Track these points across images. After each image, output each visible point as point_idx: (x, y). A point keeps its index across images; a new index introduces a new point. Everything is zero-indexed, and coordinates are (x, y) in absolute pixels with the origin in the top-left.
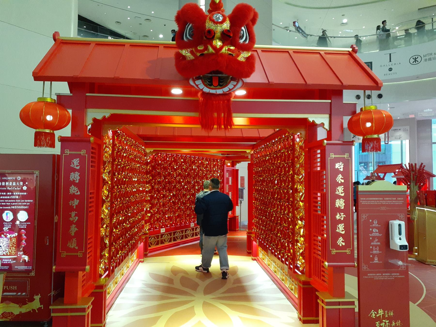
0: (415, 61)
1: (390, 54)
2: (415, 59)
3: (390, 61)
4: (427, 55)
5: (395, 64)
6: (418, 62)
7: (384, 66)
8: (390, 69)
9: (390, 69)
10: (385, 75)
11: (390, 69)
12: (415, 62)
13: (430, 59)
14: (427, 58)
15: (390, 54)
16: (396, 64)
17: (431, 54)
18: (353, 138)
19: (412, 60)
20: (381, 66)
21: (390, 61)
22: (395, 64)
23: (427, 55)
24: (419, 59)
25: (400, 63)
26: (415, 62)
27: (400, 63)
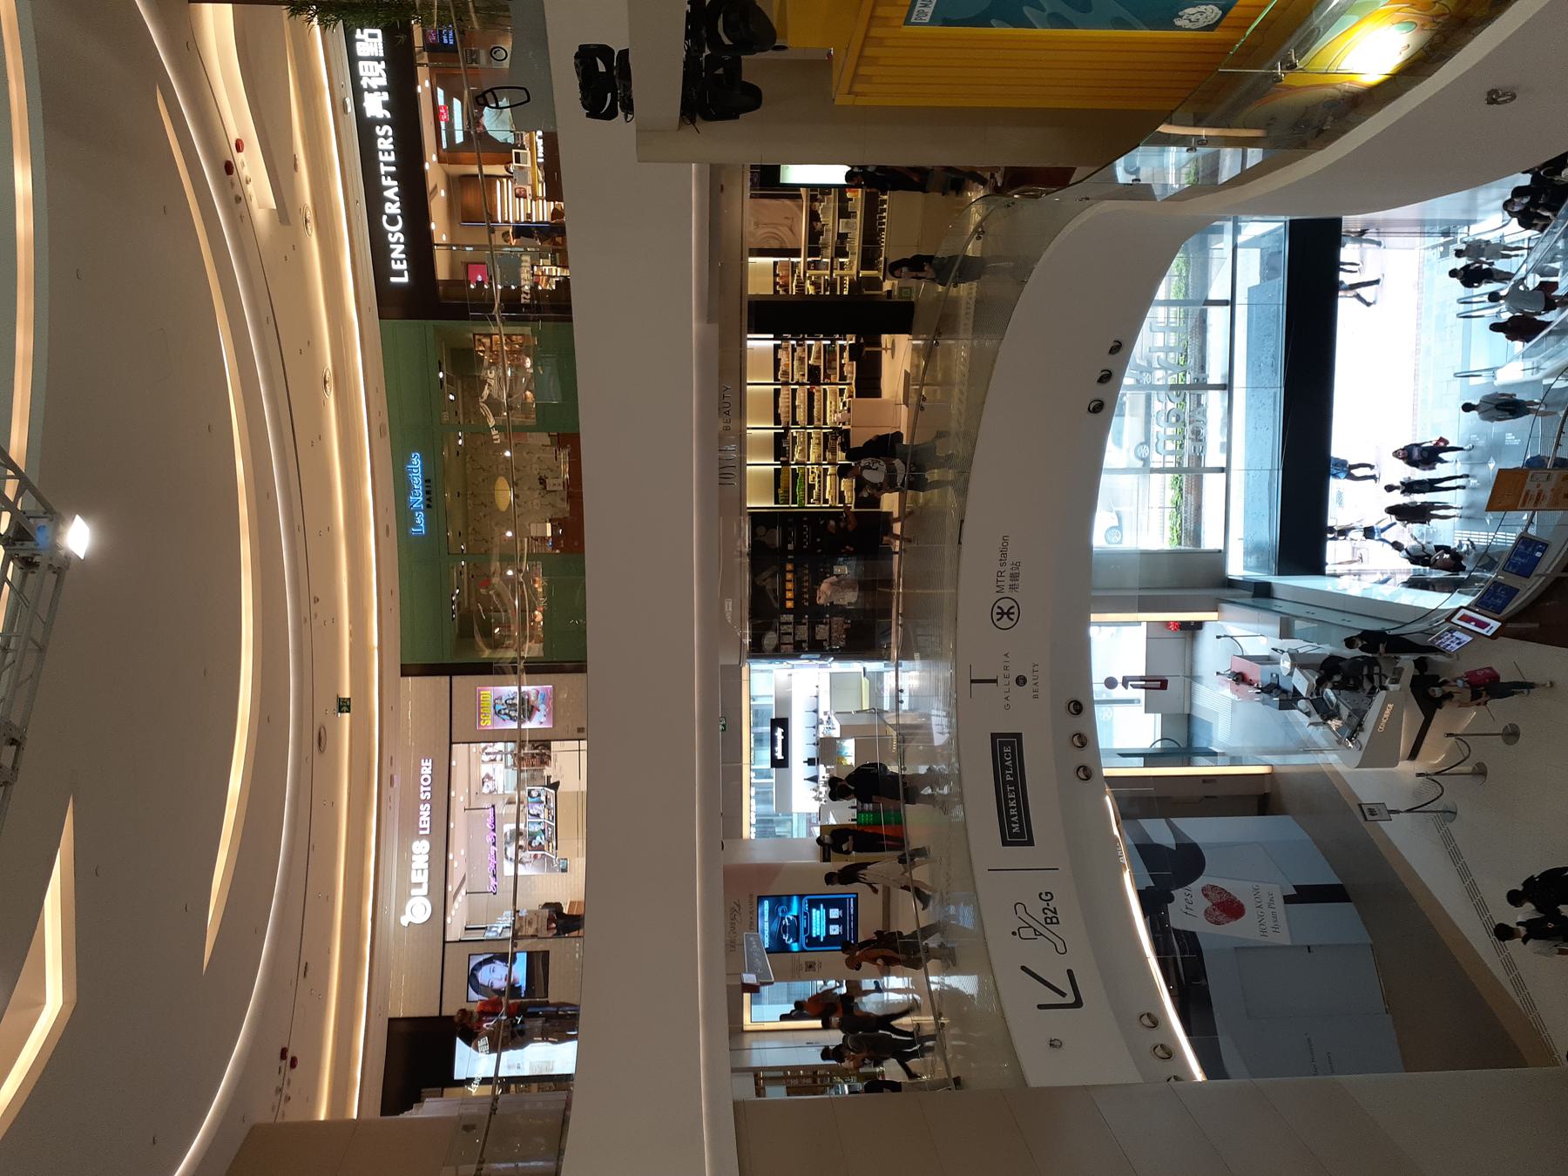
0: (1008, 613)
1: (972, 681)
2: (1008, 613)
3: (995, 681)
4: (999, 583)
5: (1006, 668)
6: (1013, 607)
7: (1007, 698)
8: (1021, 681)
9: (1021, 681)
10: (1035, 697)
11: (1021, 681)
12: (998, 614)
13: (1014, 577)
14: (1007, 582)
15: (972, 681)
16: (1006, 664)
17: (1000, 574)
19: (1005, 622)
20: (1007, 707)
21: (995, 681)
22: (1006, 668)
23: (999, 583)
24: (1005, 605)
25: (1006, 655)
26: (998, 614)
27: (1006, 655)
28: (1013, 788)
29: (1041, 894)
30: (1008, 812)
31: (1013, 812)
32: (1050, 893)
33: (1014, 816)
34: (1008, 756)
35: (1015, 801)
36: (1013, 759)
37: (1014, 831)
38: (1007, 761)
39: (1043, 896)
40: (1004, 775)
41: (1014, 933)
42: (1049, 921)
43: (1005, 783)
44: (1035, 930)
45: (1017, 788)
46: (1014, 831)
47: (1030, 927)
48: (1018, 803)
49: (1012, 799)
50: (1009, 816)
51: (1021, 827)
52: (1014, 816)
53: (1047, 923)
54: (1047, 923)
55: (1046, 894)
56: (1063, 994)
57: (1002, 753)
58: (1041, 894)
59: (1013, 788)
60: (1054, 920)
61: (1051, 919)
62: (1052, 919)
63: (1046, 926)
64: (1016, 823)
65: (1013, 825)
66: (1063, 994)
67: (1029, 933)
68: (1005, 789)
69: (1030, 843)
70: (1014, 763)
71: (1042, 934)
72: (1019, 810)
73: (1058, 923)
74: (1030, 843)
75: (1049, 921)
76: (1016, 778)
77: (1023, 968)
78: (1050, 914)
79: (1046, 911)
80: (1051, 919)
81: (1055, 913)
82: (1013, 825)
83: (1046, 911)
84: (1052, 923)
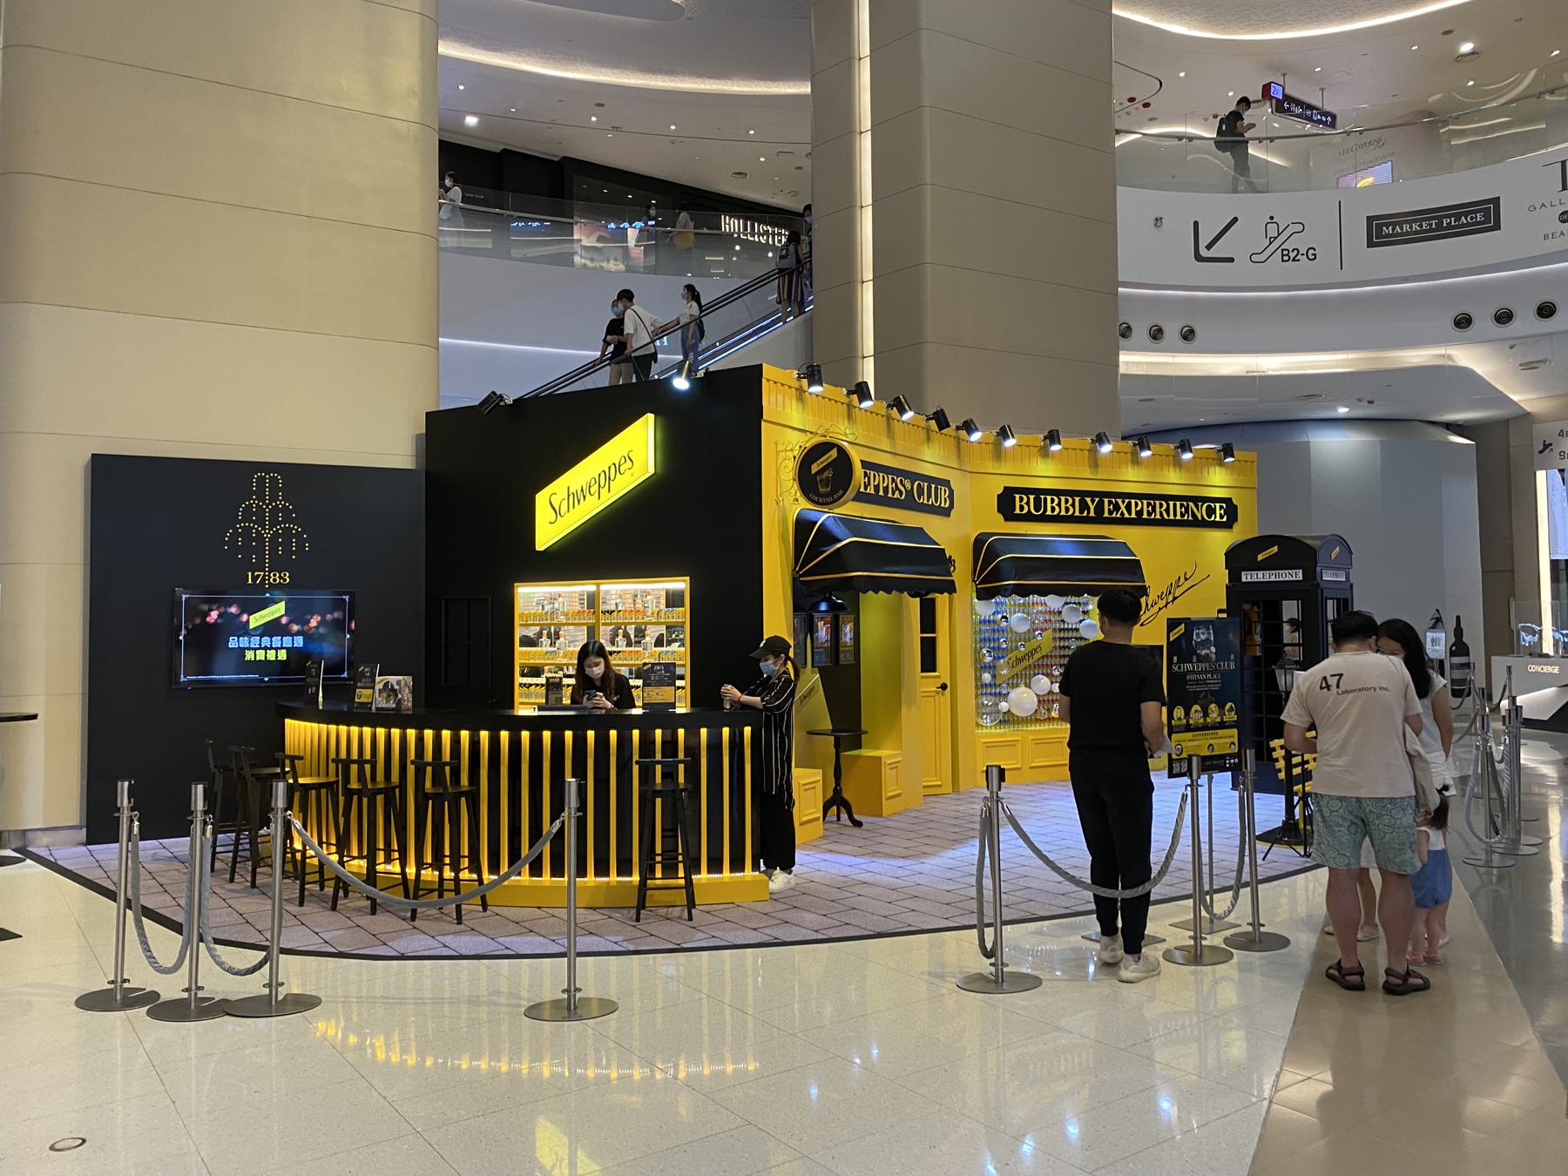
7: (1543, 205)
10: (1546, 237)
18: (1540, 452)
28: (1434, 226)
29: (1315, 250)
30: (1406, 222)
31: (1406, 227)
32: (1315, 258)
33: (1402, 229)
34: (1472, 218)
35: (1418, 229)
36: (1468, 224)
37: (1384, 228)
38: (1466, 219)
39: (1311, 251)
40: (1449, 216)
41: (1272, 218)
42: (1285, 252)
43: (1440, 219)
44: (1276, 238)
45: (1434, 230)
46: (1384, 228)
47: (1279, 235)
48: (1417, 232)
49: (1421, 226)
50: (1401, 224)
51: (1388, 235)
52: (1402, 229)
53: (1283, 250)
54: (1283, 250)
55: (1315, 255)
56: (1209, 247)
57: (1475, 212)
58: (1315, 250)
59: (1434, 226)
60: (1286, 258)
61: (1288, 255)
62: (1286, 256)
63: (1280, 249)
64: (1393, 230)
65: (1390, 228)
66: (1209, 247)
67: (1272, 232)
68: (1434, 218)
69: (1370, 244)
70: (1463, 225)
71: (1271, 243)
72: (1407, 233)
73: (1283, 261)
74: (1370, 244)
75: (1285, 252)
76: (1445, 229)
77: (1235, 220)
78: (1292, 255)
79: (1296, 252)
80: (1288, 255)
81: (1294, 260)
82: (1390, 228)
83: (1296, 252)
84: (1283, 255)
